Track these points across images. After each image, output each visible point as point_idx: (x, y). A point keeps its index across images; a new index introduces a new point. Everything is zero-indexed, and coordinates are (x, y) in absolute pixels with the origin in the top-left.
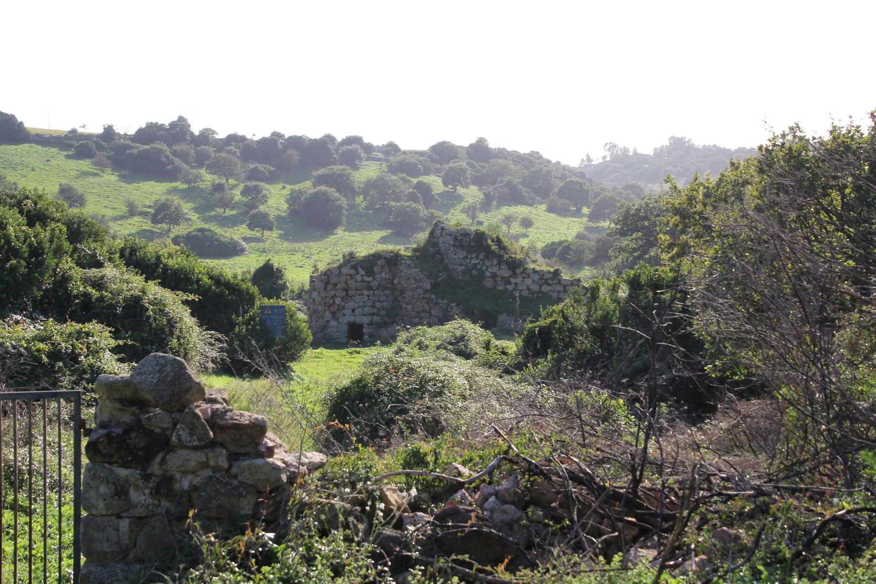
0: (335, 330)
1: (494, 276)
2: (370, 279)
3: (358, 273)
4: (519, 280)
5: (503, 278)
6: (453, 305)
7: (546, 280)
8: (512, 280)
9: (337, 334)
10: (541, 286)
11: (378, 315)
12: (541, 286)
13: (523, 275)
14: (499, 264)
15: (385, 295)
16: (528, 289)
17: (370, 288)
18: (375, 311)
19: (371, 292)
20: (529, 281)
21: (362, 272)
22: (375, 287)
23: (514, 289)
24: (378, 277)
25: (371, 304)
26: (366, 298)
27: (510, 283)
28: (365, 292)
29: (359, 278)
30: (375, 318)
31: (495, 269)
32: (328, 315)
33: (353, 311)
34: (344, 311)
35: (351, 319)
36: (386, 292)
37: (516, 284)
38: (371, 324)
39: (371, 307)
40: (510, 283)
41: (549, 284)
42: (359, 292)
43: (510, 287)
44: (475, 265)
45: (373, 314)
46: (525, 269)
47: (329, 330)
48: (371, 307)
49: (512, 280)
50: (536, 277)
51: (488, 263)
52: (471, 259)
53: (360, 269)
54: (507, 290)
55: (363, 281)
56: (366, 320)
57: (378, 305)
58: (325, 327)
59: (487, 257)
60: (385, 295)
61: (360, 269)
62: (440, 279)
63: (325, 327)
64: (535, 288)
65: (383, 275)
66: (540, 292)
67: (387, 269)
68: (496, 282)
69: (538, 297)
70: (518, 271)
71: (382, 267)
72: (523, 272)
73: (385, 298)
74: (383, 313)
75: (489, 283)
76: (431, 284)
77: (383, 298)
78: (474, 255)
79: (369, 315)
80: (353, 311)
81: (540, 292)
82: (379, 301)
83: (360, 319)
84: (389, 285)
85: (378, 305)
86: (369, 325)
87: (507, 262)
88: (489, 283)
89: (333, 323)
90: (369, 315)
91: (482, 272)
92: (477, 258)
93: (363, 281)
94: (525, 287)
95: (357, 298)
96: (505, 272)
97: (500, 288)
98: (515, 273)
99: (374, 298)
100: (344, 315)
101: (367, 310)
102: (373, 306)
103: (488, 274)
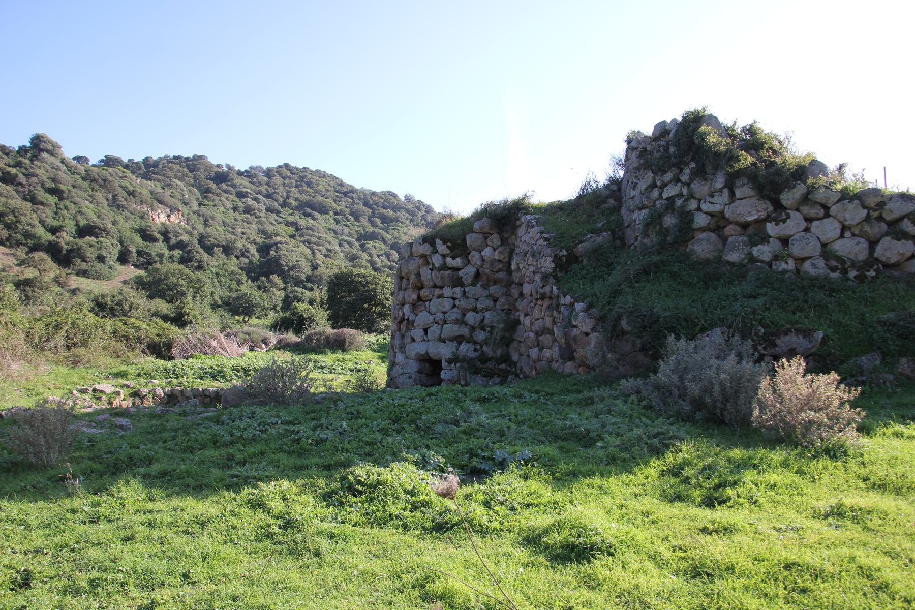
1: (719, 223)
2: (458, 262)
3: (435, 251)
4: (793, 225)
5: (745, 226)
6: (579, 306)
7: (893, 224)
8: (770, 228)
10: (873, 244)
11: (470, 340)
12: (873, 244)
13: (806, 210)
14: (730, 186)
15: (489, 296)
16: (826, 251)
17: (458, 282)
18: (465, 331)
19: (458, 290)
20: (828, 229)
21: (441, 247)
22: (468, 280)
23: (776, 258)
24: (475, 257)
25: (454, 315)
26: (447, 304)
27: (765, 239)
28: (447, 292)
29: (437, 260)
31: (719, 203)
33: (426, 331)
36: (493, 289)
37: (785, 241)
39: (456, 322)
40: (765, 239)
41: (902, 236)
42: (437, 292)
43: (763, 252)
44: (671, 200)
45: (459, 339)
46: (812, 189)
48: (456, 322)
49: (770, 228)
50: (854, 214)
51: (701, 189)
52: (665, 185)
53: (438, 242)
54: (752, 259)
55: (444, 267)
57: (471, 318)
59: (700, 173)
60: (489, 296)
61: (438, 242)
62: (581, 248)
64: (851, 248)
65: (487, 252)
66: (871, 261)
67: (495, 239)
68: (724, 240)
69: (861, 278)
70: (788, 198)
71: (486, 236)
72: (806, 199)
73: (489, 303)
75: (702, 247)
76: (556, 259)
77: (483, 303)
78: (668, 176)
79: (452, 340)
80: (426, 331)
81: (871, 261)
82: (475, 310)
84: (501, 275)
85: (471, 318)
86: (450, 362)
87: (750, 174)
88: (702, 247)
91: (686, 218)
92: (677, 180)
93: (444, 267)
94: (811, 247)
95: (434, 305)
96: (749, 208)
97: (734, 257)
98: (778, 206)
99: (461, 303)
101: (450, 330)
102: (461, 322)
103: (701, 220)
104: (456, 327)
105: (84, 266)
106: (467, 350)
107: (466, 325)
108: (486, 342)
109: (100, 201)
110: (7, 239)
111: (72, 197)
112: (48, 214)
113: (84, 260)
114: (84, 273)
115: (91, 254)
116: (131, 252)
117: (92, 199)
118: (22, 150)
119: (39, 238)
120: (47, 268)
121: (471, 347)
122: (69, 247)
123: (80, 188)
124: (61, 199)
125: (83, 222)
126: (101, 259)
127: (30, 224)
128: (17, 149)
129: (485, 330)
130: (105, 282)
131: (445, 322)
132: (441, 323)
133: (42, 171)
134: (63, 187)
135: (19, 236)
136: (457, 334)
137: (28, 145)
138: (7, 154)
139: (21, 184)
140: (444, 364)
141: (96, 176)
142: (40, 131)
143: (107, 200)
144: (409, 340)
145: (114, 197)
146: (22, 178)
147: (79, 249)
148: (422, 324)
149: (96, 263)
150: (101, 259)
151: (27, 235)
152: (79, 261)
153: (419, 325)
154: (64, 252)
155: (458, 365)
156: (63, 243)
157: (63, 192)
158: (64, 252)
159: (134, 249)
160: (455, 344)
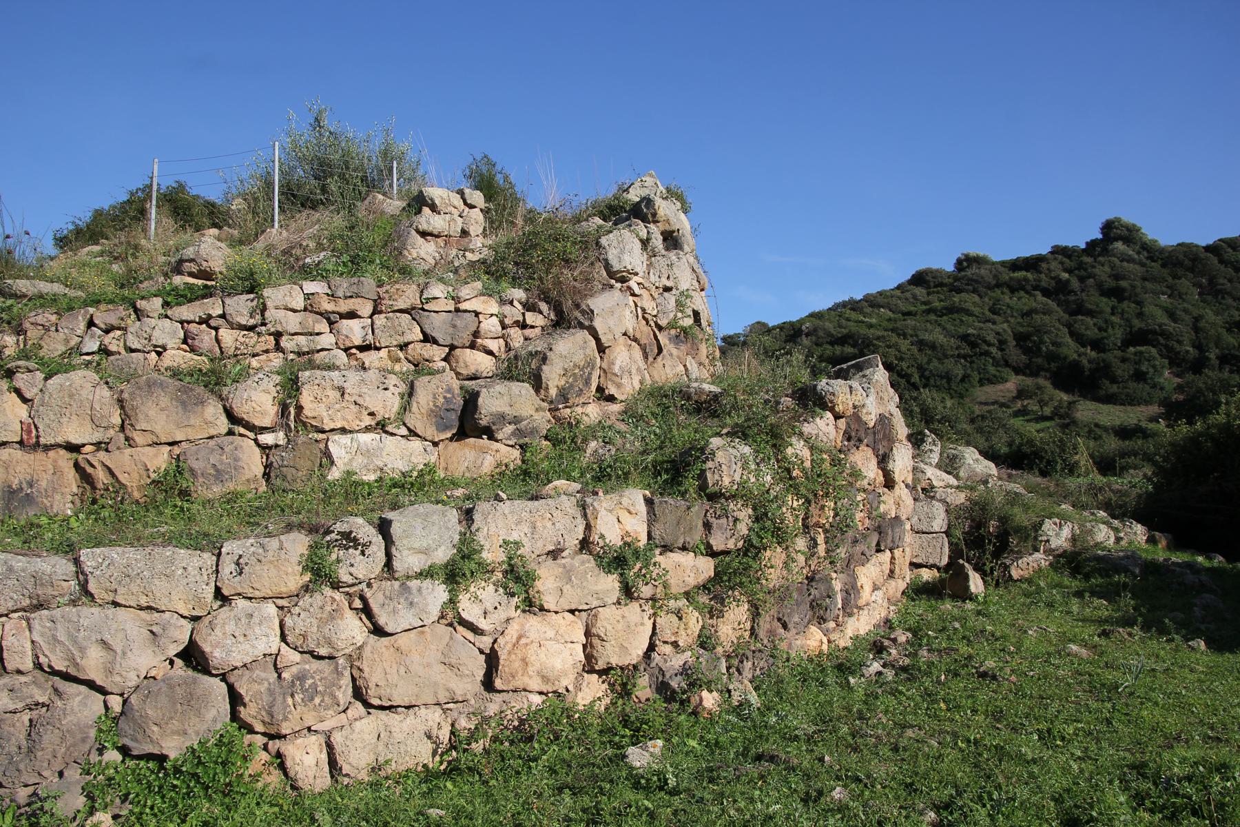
105: (1114, 389)
109: (1183, 290)
110: (1027, 366)
111: (1136, 295)
112: (1088, 326)
113: (1114, 380)
114: (1110, 399)
115: (1121, 371)
116: (1208, 359)
117: (1173, 292)
118: (1092, 245)
119: (1066, 358)
120: (1046, 398)
122: (1094, 366)
123: (1153, 279)
124: (1121, 300)
125: (1138, 324)
126: (1140, 376)
127: (1054, 344)
128: (1083, 246)
130: (1142, 408)
133: (1107, 269)
134: (1124, 284)
135: (1039, 360)
137: (1100, 236)
138: (1069, 257)
139: (1073, 291)
141: (1181, 257)
142: (1111, 217)
143: (1200, 286)
145: (1212, 281)
146: (1075, 284)
147: (1108, 366)
149: (1132, 385)
150: (1140, 376)
151: (1052, 357)
152: (1107, 382)
154: (1087, 373)
156: (1085, 362)
157: (1124, 290)
158: (1087, 373)
159: (1212, 355)
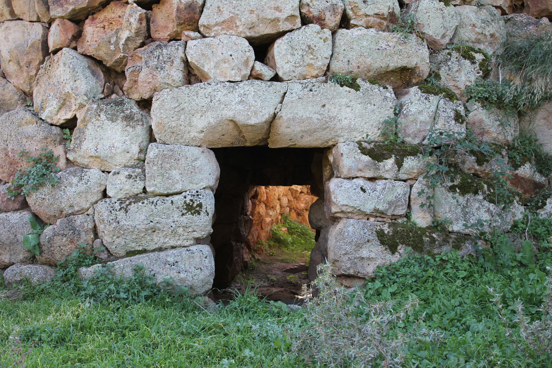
0: (120, 186)
9: (139, 215)
11: (430, 85)
18: (417, 56)
30: (416, 103)
32: (69, 80)
33: (262, 47)
34: (195, 49)
35: (248, 107)
38: (386, 148)
45: (401, 79)
47: (74, 192)
56: (349, 119)
58: (46, 168)
63: (46, 168)
74: (463, 75)
79: (379, 78)
80: (262, 47)
83: (302, 114)
86: (376, 153)
89: (109, 138)
90: (379, 78)
100: (192, 75)
101: (365, 48)
104: (389, 40)
106: (435, 118)
107: (421, 36)
108: (469, 95)
121: (448, 109)
129: (472, 60)
131: (345, 22)
132: (333, 20)
136: (396, 62)
140: (348, 158)
144: (177, 73)
148: (245, 18)
153: (229, 24)
155: (410, 163)
160: (390, 94)
